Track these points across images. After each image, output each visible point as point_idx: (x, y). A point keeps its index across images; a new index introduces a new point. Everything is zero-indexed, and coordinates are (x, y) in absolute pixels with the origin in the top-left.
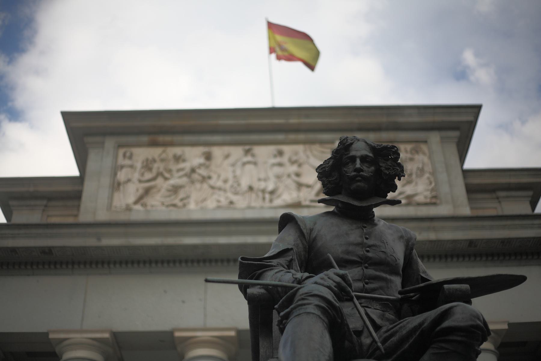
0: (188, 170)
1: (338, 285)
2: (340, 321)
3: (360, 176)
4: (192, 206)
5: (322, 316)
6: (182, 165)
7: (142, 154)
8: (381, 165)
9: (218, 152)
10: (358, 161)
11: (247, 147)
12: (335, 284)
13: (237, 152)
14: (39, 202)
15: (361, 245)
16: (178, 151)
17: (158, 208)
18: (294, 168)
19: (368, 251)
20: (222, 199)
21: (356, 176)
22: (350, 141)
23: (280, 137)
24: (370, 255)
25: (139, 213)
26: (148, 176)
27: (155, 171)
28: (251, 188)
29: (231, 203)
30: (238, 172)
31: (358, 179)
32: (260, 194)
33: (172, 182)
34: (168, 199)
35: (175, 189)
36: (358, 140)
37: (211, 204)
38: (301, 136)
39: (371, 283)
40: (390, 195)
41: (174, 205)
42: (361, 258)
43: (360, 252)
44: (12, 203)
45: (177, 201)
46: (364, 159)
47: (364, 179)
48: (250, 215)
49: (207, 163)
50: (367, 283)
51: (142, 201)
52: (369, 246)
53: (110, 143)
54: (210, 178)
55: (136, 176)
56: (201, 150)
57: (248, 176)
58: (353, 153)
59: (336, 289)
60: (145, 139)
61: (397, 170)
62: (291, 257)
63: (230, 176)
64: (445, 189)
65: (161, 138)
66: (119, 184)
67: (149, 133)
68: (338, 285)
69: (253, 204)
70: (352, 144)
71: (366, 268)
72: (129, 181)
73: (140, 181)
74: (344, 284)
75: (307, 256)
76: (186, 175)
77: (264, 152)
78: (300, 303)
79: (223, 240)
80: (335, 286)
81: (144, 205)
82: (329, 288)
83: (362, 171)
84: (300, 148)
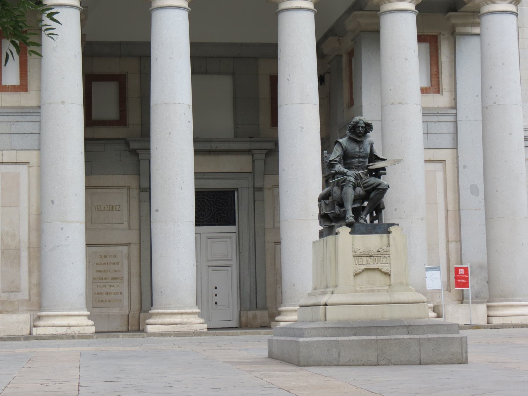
46: (362, 127)
58: (359, 125)
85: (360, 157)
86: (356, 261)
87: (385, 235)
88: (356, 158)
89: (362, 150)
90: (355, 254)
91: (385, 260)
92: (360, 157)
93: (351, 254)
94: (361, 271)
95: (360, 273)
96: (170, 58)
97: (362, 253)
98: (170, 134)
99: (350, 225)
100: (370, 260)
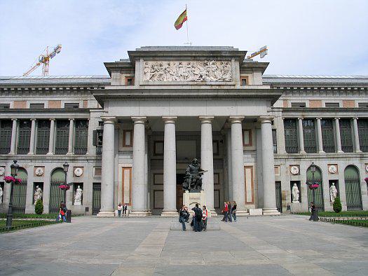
7: (151, 63)
9: (172, 63)
13: (177, 63)
16: (159, 62)
17: (156, 80)
25: (151, 82)
35: (161, 75)
37: (170, 80)
56: (167, 62)
57: (182, 71)
64: (234, 76)
65: (156, 58)
77: (184, 63)
84: (195, 62)
99: (189, 190)
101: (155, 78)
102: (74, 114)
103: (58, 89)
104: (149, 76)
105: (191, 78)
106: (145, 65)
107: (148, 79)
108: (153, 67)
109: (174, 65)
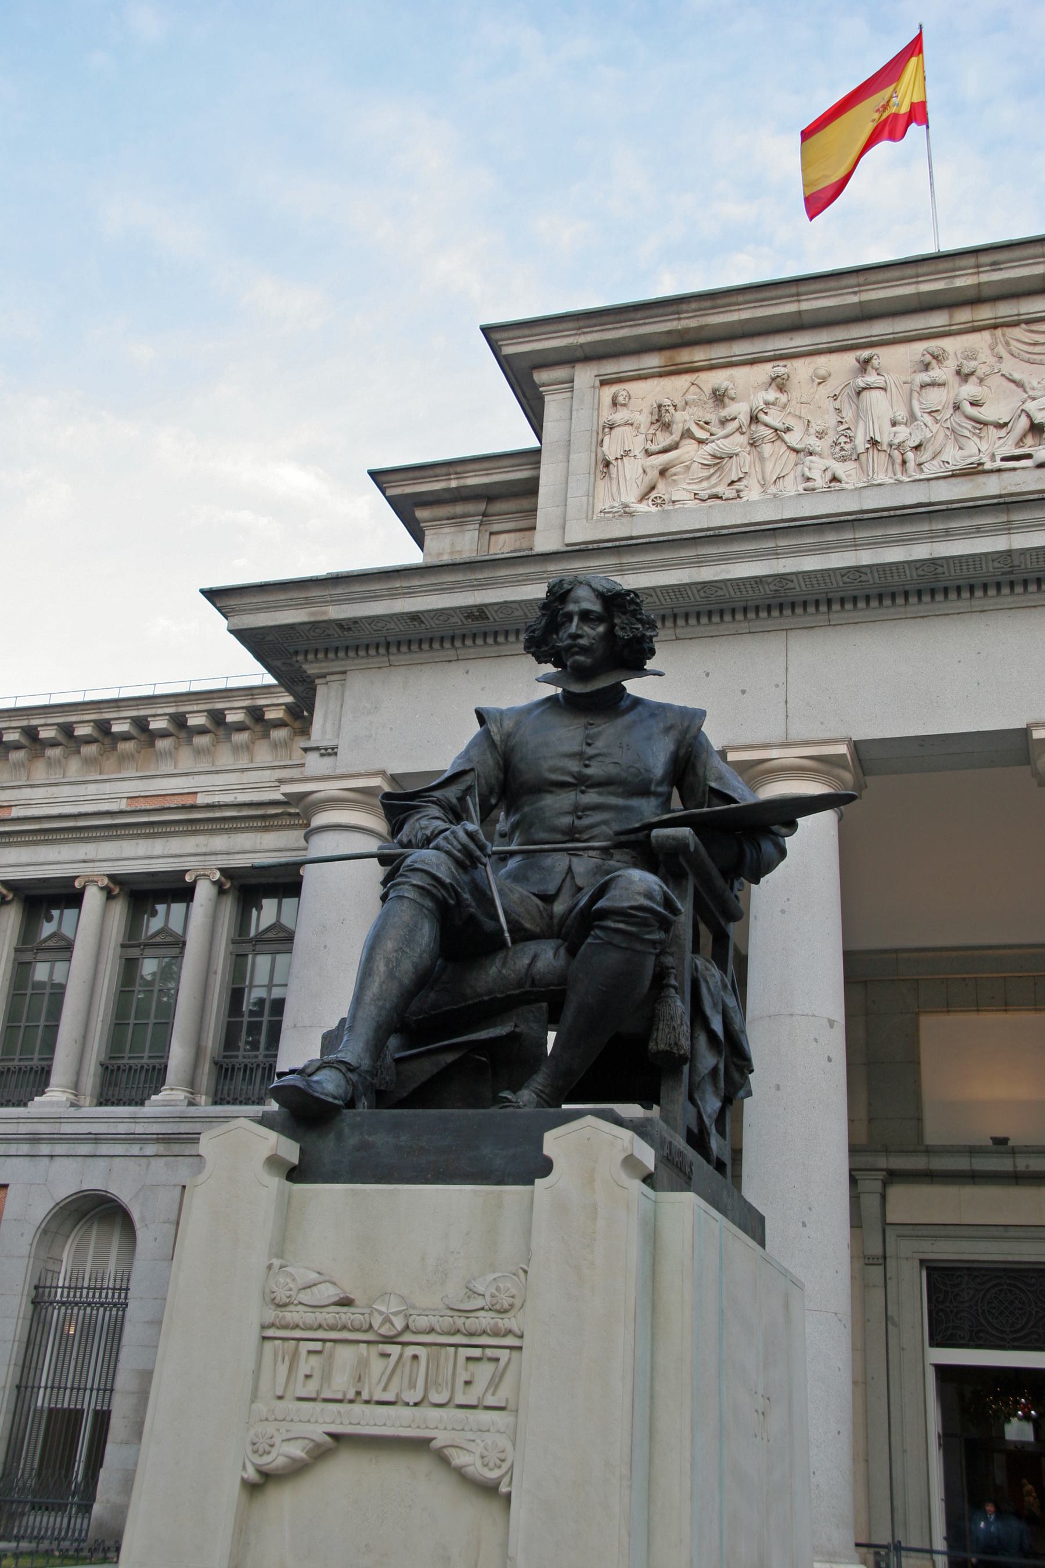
0: (744, 418)
1: (465, 849)
2: (452, 902)
3: (576, 645)
4: (753, 493)
5: (419, 900)
6: (732, 409)
7: (647, 394)
8: (617, 621)
9: (801, 370)
10: (576, 619)
11: (865, 354)
12: (459, 847)
14: (471, 508)
15: (580, 755)
18: (970, 390)
19: (586, 766)
20: (816, 474)
21: (569, 648)
22: (566, 587)
23: (938, 320)
24: (589, 771)
25: (649, 521)
26: (664, 440)
27: (677, 429)
28: (874, 443)
29: (835, 479)
30: (848, 414)
31: (576, 649)
32: (896, 454)
33: (709, 448)
34: (705, 484)
35: (719, 460)
36: (581, 583)
37: (792, 487)
38: (985, 313)
39: (588, 816)
40: (649, 665)
41: (716, 497)
42: (574, 777)
43: (574, 766)
44: (421, 514)
45: (721, 489)
46: (586, 616)
47: (584, 650)
48: (873, 501)
49: (783, 398)
50: (579, 818)
51: (653, 495)
52: (591, 758)
53: (585, 376)
54: (788, 430)
55: (637, 444)
56: (767, 370)
58: (572, 607)
59: (459, 855)
60: (652, 361)
61: (638, 629)
62: (469, 783)
63: (832, 420)
65: (685, 356)
66: (607, 464)
67: (661, 349)
68: (465, 849)
69: (881, 478)
70: (569, 591)
71: (583, 792)
72: (627, 453)
73: (648, 453)
74: (472, 846)
75: (501, 776)
76: (739, 430)
78: (399, 880)
79: (811, 563)
80: (459, 851)
81: (659, 502)
82: (448, 853)
83: (580, 636)
85: (582, 782)
86: (283, 1369)
87: (513, 1192)
88: (563, 785)
89: (600, 744)
90: (271, 1315)
91: (484, 1372)
92: (582, 782)
93: (255, 1312)
94: (297, 1451)
95: (296, 1470)
96: (783, 912)
97: (328, 1316)
98: (778, 1088)
100: (377, 1366)
101: (680, 491)
102: (219, 842)
103: (179, 721)
104: (632, 475)
105: (955, 457)
106: (607, 414)
107: (630, 496)
108: (661, 421)
109: (818, 377)
